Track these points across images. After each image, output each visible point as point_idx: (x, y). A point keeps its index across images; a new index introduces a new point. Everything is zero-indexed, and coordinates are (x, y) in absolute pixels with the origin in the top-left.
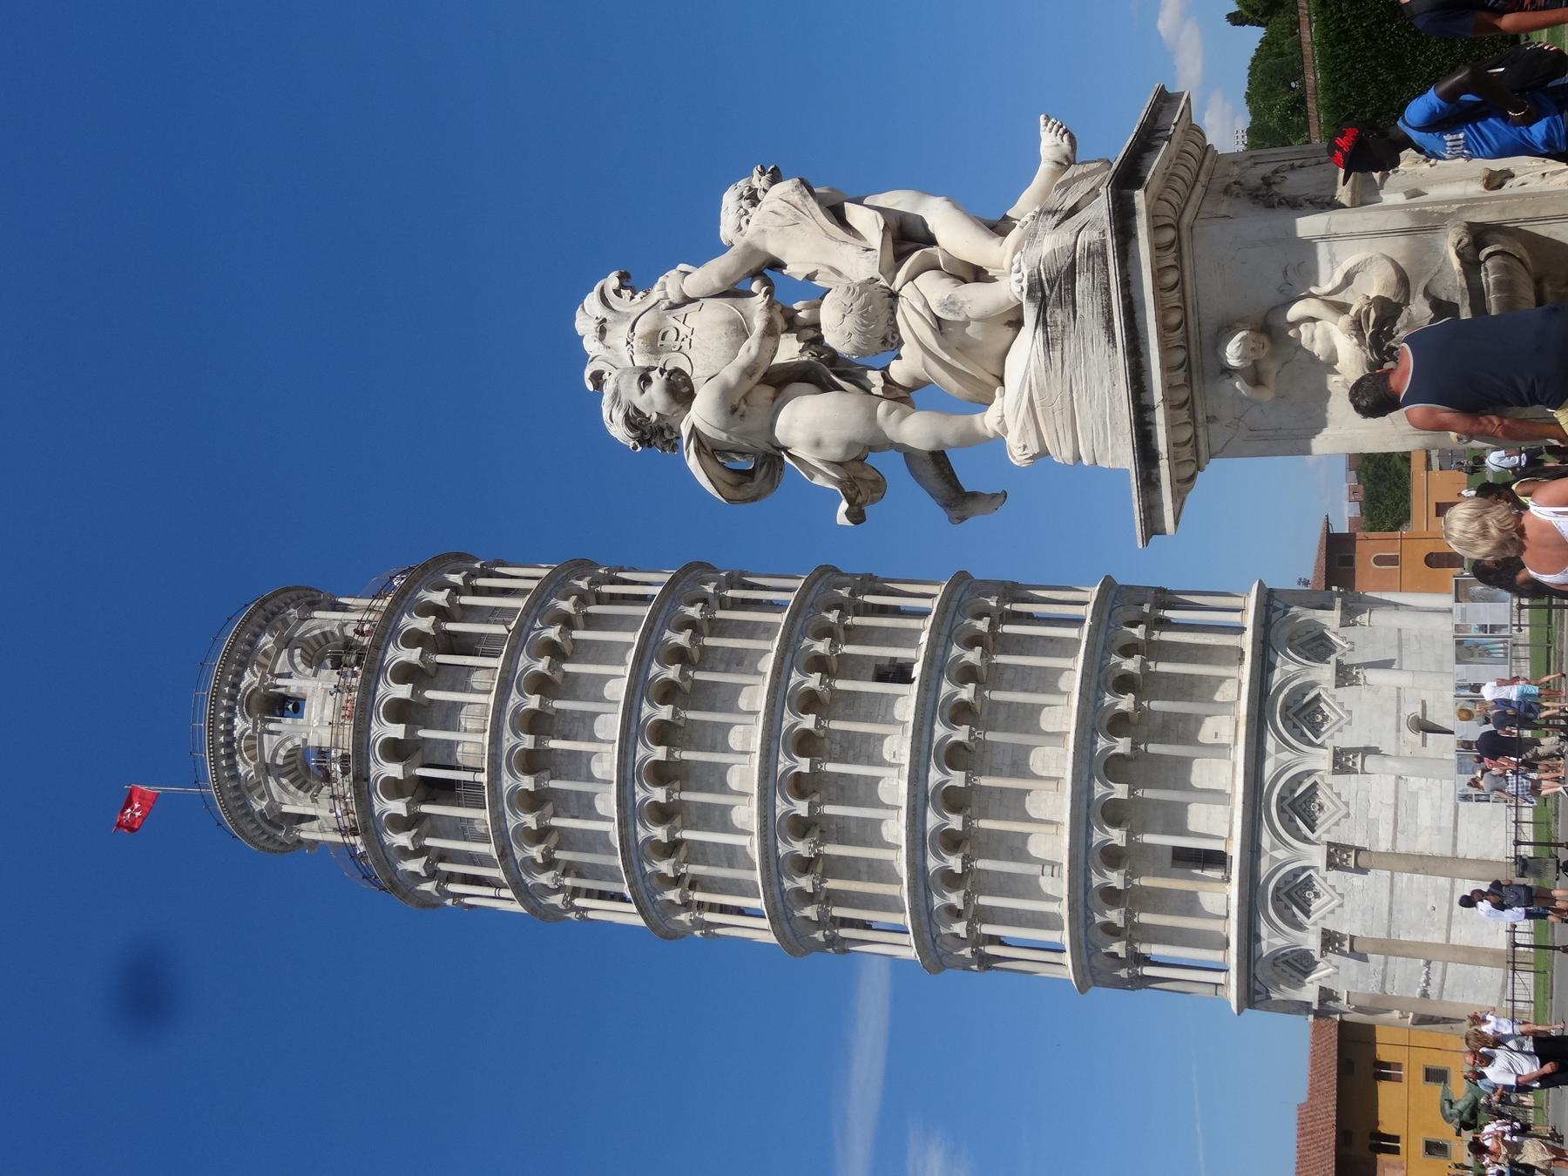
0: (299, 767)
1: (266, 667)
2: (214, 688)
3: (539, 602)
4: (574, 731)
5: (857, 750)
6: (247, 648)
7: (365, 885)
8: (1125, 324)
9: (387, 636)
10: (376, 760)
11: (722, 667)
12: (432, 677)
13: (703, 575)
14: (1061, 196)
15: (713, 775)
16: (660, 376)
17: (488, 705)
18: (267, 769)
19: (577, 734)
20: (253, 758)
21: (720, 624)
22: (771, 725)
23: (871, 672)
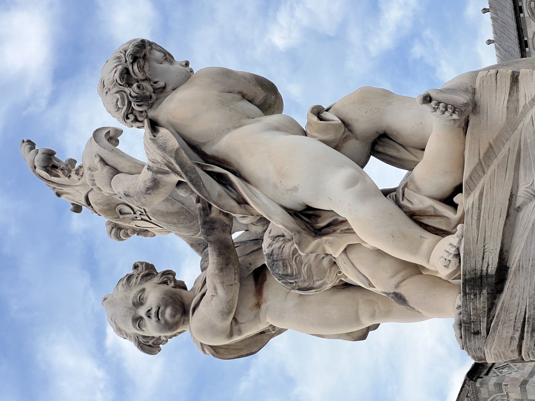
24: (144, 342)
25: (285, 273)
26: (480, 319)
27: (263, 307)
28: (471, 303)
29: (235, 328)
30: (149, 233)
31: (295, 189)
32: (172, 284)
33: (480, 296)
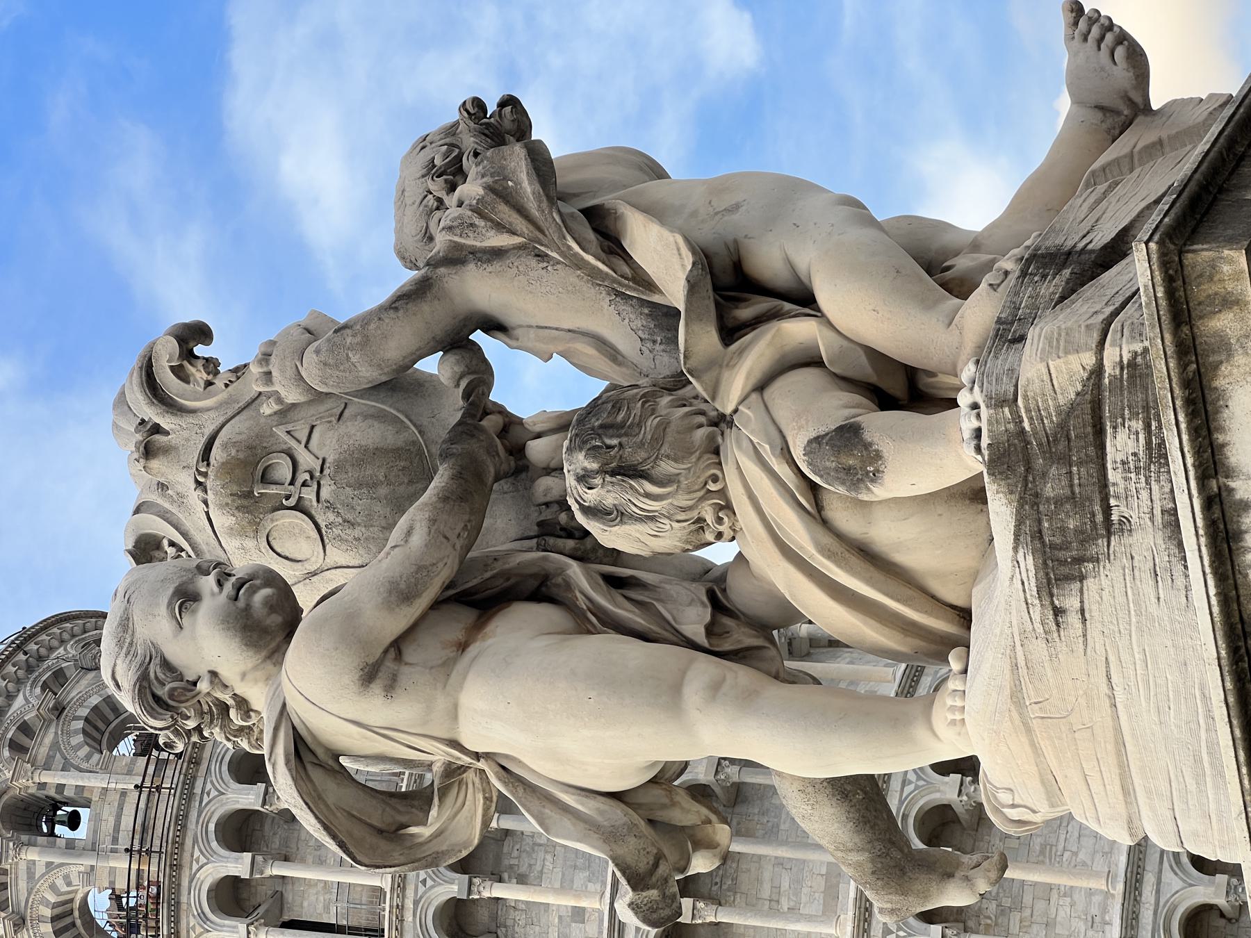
0: (78, 922)
4: (538, 868)
5: (1027, 913)
8: (1211, 566)
10: (203, 916)
14: (1092, 209)
16: (216, 589)
19: (541, 872)
24: (157, 678)
25: (609, 420)
27: (473, 650)
28: (1030, 289)
29: (389, 664)
31: (736, 207)
33: (1054, 278)
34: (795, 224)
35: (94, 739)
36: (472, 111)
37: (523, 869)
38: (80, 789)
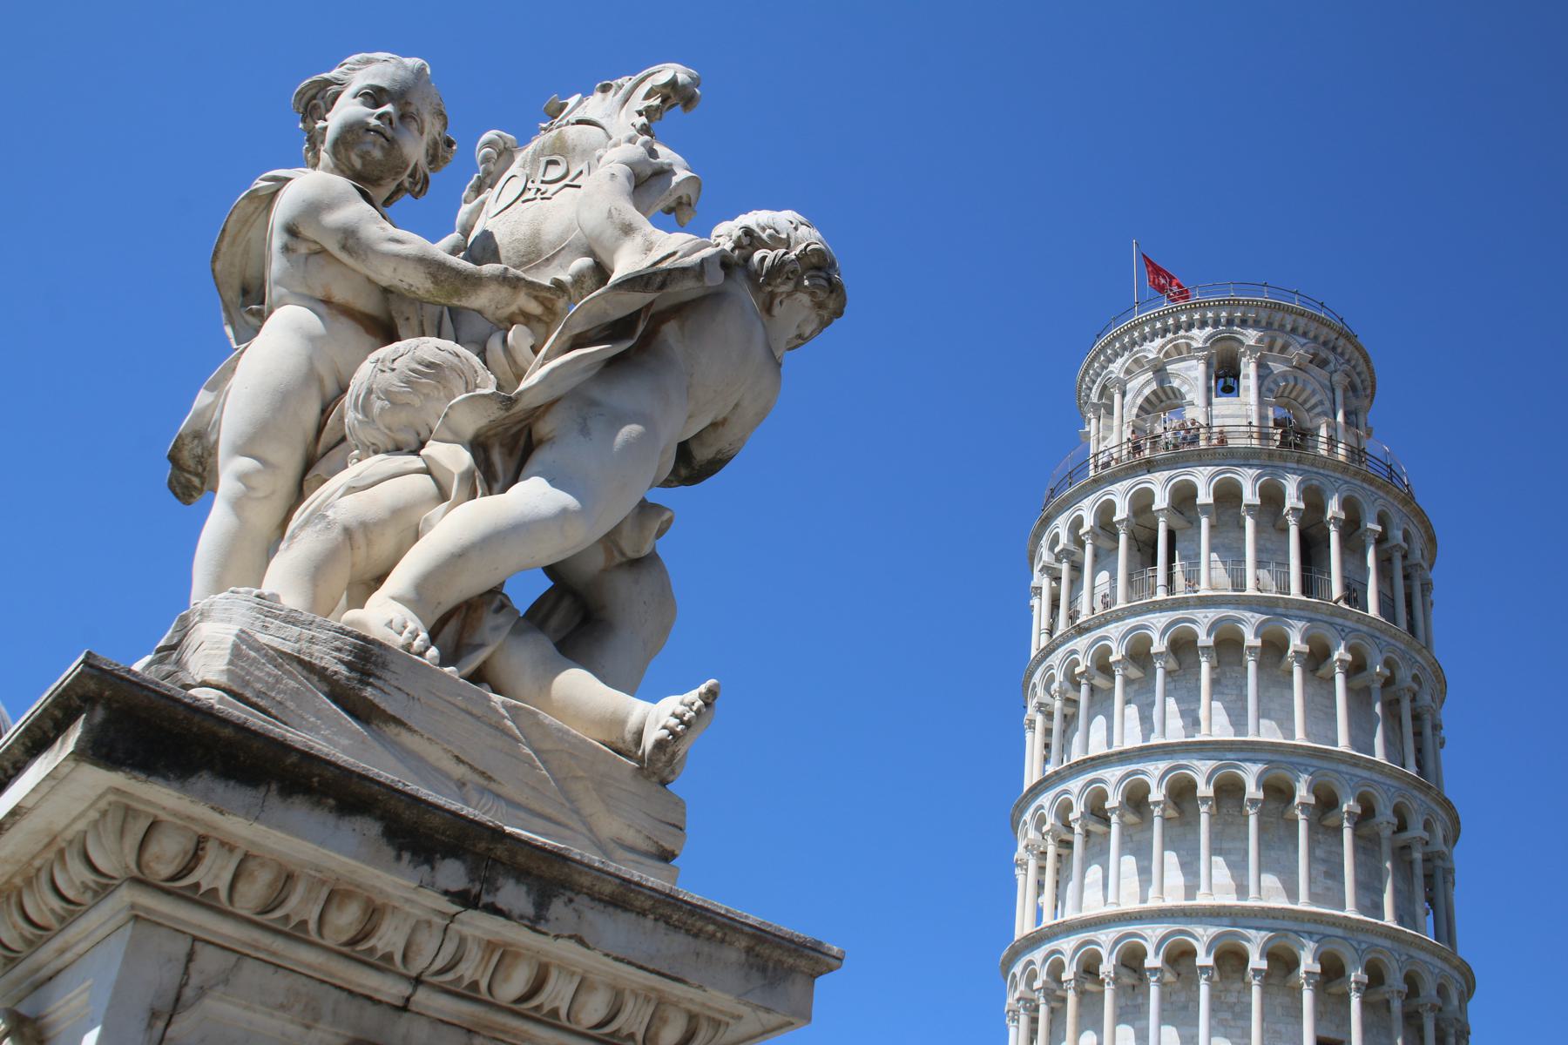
0: (1163, 404)
1: (1271, 349)
2: (1239, 300)
3: (1378, 634)
4: (1226, 691)
5: (1232, 1023)
6: (1289, 327)
7: (1047, 492)
9: (1315, 470)
11: (1319, 853)
12: (1274, 526)
13: (1438, 823)
15: (1187, 854)
17: (1244, 591)
18: (1160, 371)
19: (1223, 693)
20: (1167, 354)
21: (1377, 848)
22: (1249, 915)
23: (1331, 1034)
26: (289, 641)
30: (473, 194)
32: (407, 185)
33: (335, 658)
34: (554, 479)
35: (1283, 392)
36: (809, 249)
37: (1224, 681)
38: (1247, 389)
